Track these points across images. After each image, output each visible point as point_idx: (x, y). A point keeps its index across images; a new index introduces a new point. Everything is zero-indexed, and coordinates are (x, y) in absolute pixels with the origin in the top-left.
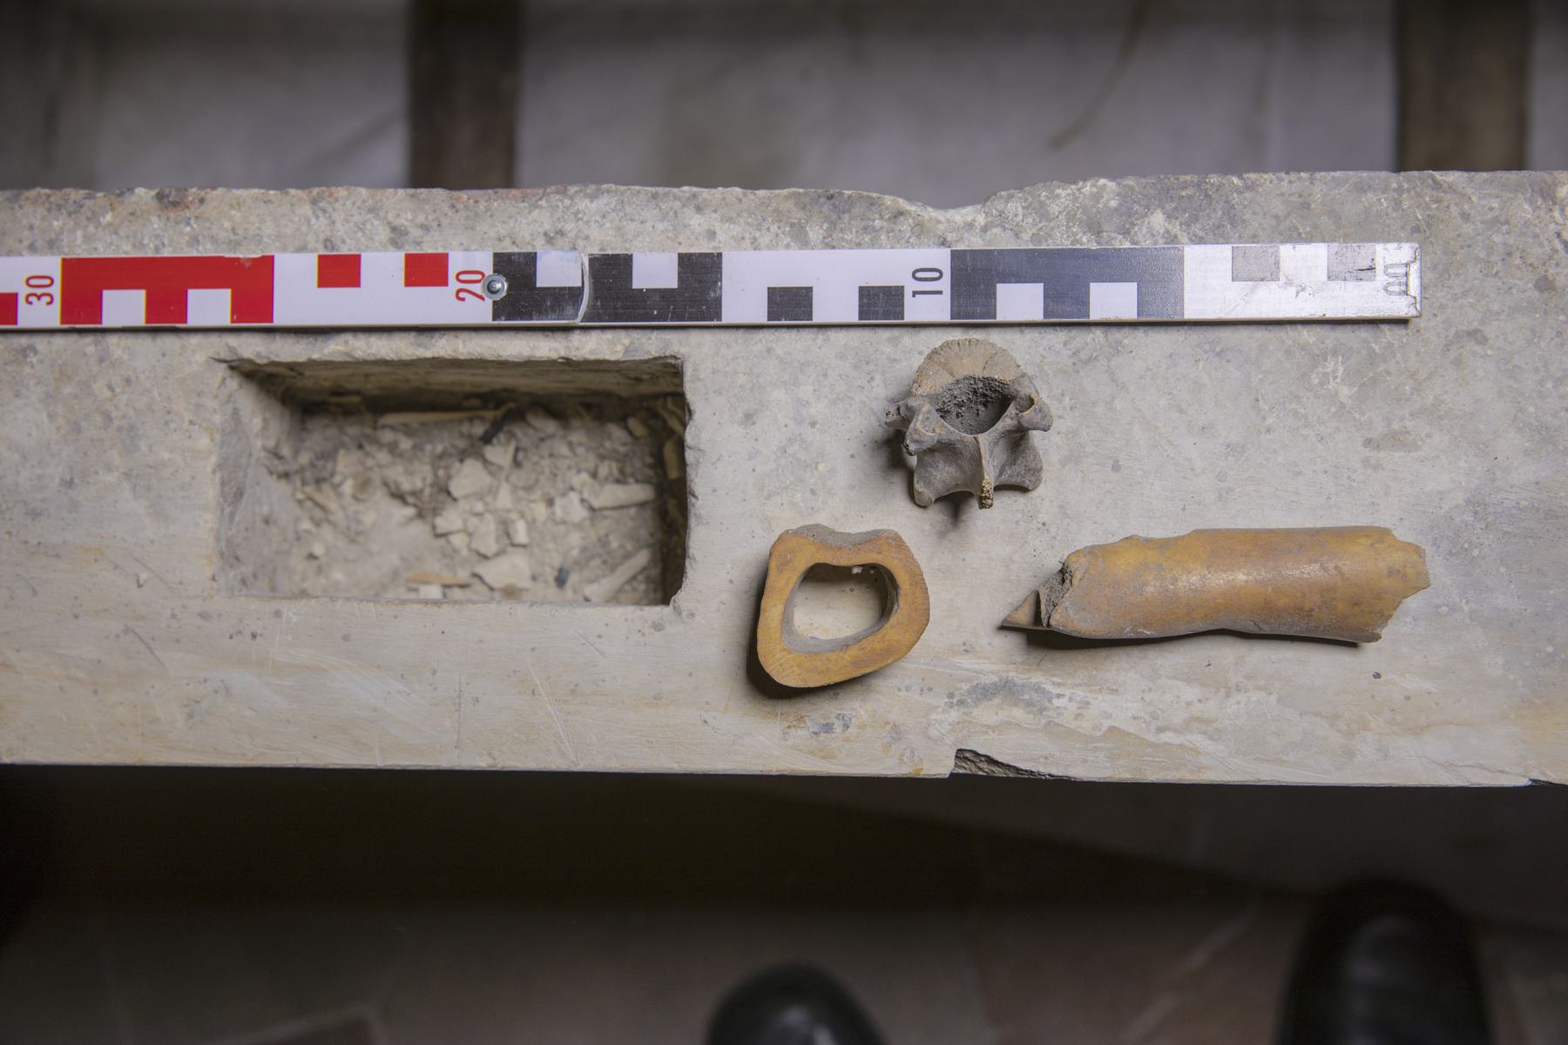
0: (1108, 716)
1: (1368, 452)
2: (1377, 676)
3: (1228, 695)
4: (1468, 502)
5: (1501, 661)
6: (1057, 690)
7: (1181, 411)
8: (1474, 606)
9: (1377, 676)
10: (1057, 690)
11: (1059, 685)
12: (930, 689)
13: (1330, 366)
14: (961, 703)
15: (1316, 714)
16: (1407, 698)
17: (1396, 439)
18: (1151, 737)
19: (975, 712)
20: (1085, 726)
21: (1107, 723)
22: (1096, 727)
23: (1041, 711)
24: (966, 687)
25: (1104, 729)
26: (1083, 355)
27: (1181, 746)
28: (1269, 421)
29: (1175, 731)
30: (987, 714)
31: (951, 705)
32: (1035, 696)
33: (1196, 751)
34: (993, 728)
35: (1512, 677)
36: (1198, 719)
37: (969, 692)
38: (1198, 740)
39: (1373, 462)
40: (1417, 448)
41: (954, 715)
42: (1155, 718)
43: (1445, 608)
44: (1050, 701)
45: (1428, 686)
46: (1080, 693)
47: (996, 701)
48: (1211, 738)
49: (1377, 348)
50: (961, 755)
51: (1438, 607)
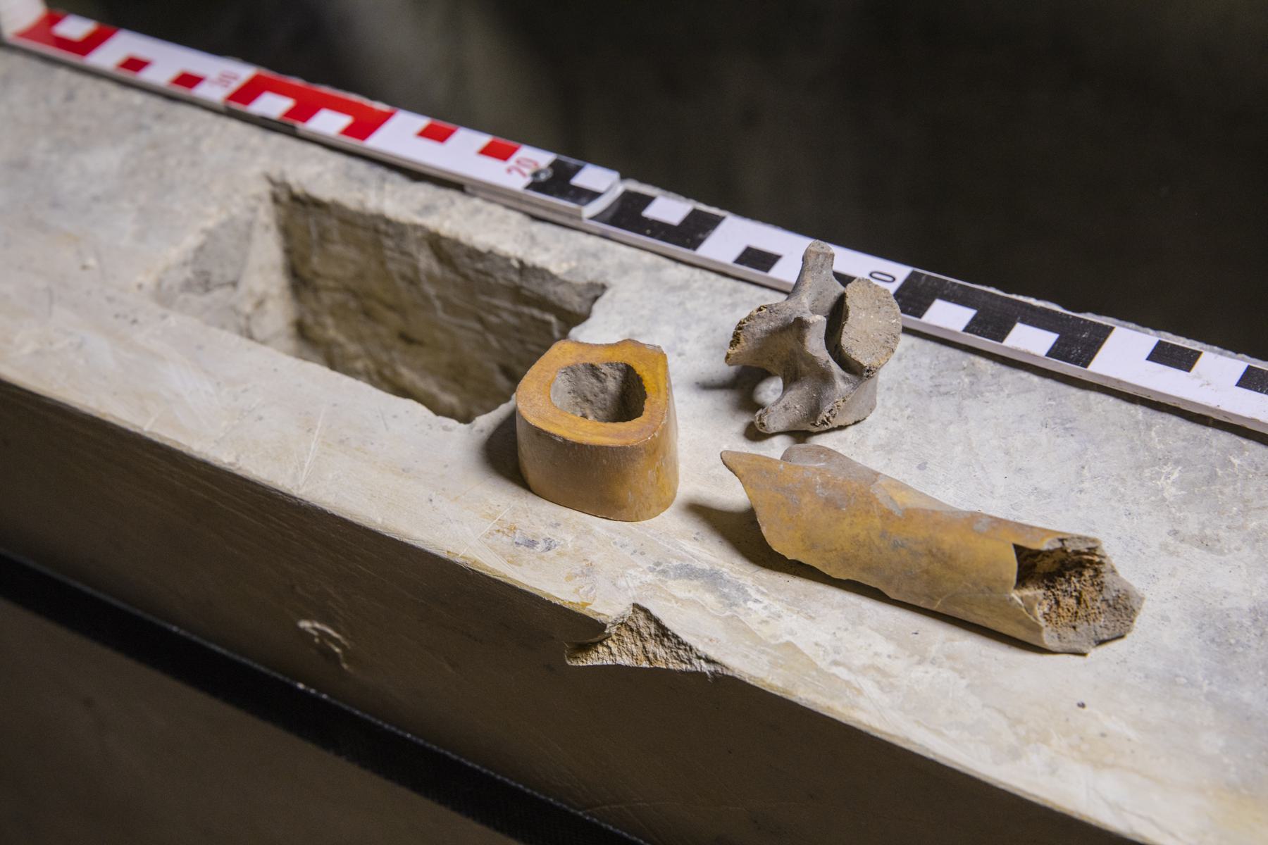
0: (792, 633)
1: (1170, 540)
2: (1082, 705)
3: (920, 663)
4: (1253, 610)
5: (1221, 742)
6: (758, 597)
7: (1007, 453)
8: (1215, 688)
9: (1082, 705)
10: (758, 597)
11: (763, 593)
12: (642, 554)
13: (1167, 469)
14: (664, 572)
15: (1000, 711)
16: (1103, 735)
17: (1205, 543)
18: (822, 665)
19: (670, 582)
20: (764, 632)
21: (787, 638)
22: (774, 636)
23: (731, 605)
24: (675, 563)
25: (781, 640)
26: (942, 389)
27: (848, 683)
28: (1086, 485)
29: (850, 669)
30: (679, 588)
31: (652, 570)
32: (734, 593)
33: (859, 692)
34: (677, 600)
35: (1226, 760)
36: (878, 670)
37: (676, 568)
38: (868, 685)
39: (1171, 548)
40: (1221, 552)
41: (650, 577)
42: (837, 652)
43: (1183, 680)
44: (745, 601)
45: (1131, 733)
46: (777, 607)
47: (695, 582)
48: (882, 689)
49: (1220, 473)
50: (637, 607)
51: (1177, 676)
